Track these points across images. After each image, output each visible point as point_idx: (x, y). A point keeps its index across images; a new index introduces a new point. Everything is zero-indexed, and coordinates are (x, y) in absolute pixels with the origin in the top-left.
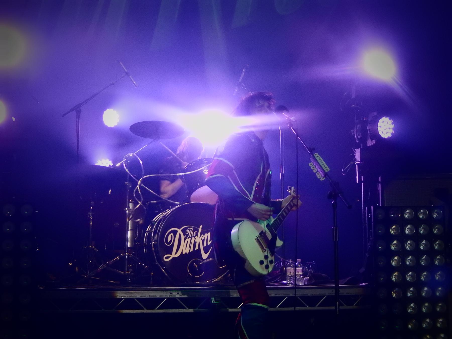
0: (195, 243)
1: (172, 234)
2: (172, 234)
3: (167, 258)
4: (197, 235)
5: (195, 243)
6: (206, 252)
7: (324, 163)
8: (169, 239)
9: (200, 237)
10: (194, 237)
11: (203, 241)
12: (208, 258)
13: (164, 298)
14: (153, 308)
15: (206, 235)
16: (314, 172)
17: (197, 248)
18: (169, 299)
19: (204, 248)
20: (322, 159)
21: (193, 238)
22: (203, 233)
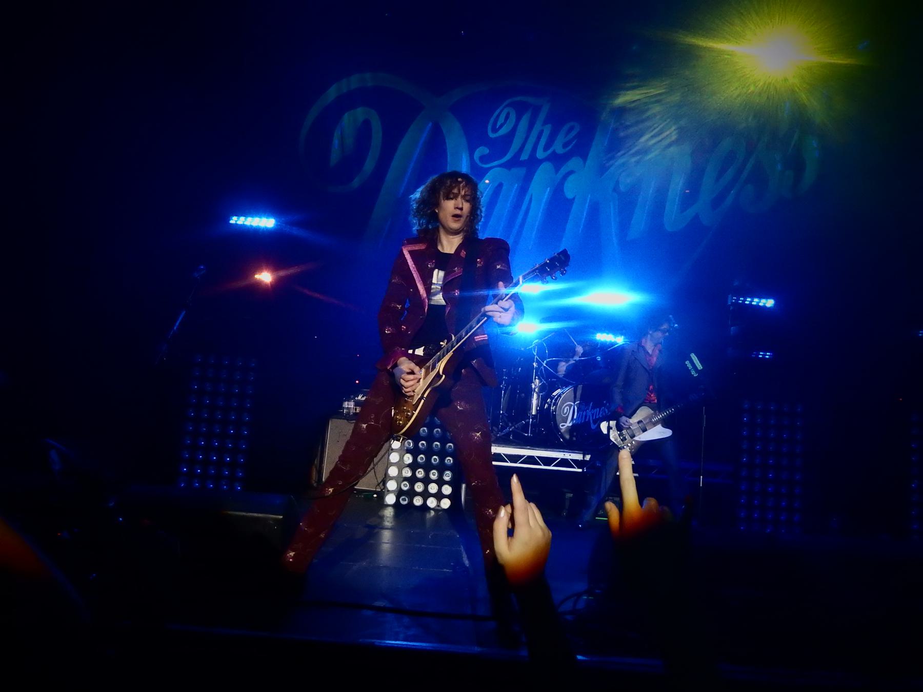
0: (586, 416)
1: (568, 407)
2: (568, 407)
3: (562, 426)
4: (588, 409)
5: (586, 416)
6: (595, 424)
7: (698, 362)
8: (565, 411)
9: (591, 410)
10: (586, 411)
11: (593, 415)
12: (596, 428)
13: (559, 458)
14: (549, 465)
15: (595, 410)
16: (690, 369)
17: (587, 420)
18: (562, 459)
19: (593, 419)
20: (697, 359)
21: (585, 412)
22: (593, 408)
